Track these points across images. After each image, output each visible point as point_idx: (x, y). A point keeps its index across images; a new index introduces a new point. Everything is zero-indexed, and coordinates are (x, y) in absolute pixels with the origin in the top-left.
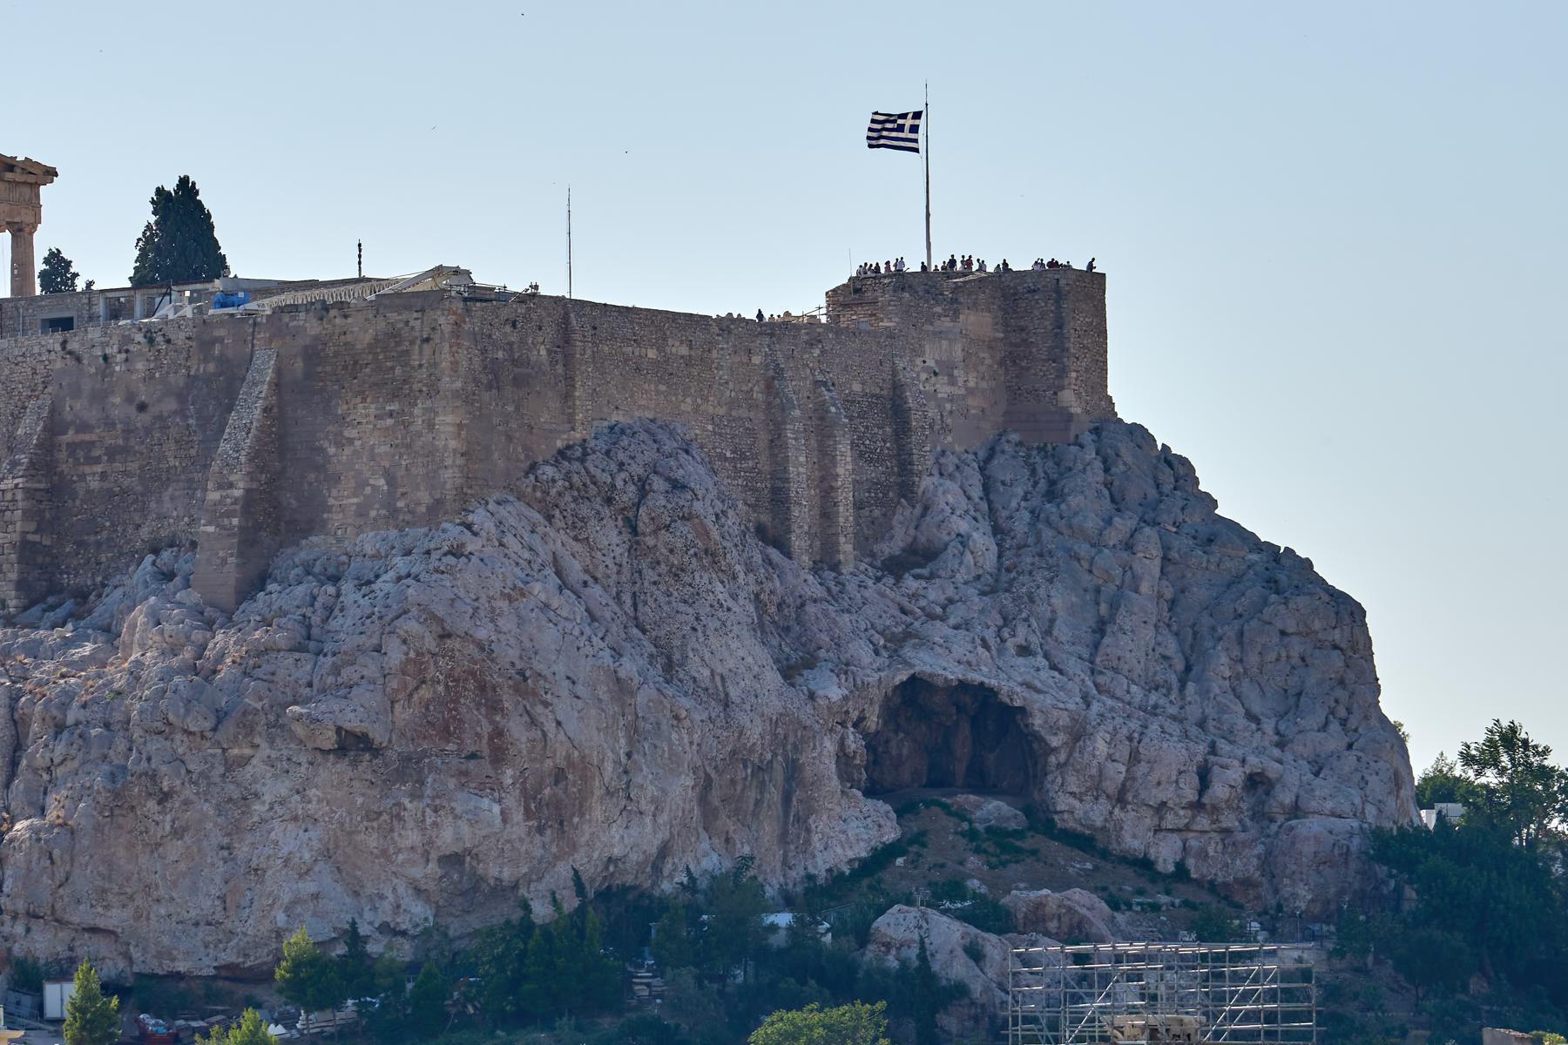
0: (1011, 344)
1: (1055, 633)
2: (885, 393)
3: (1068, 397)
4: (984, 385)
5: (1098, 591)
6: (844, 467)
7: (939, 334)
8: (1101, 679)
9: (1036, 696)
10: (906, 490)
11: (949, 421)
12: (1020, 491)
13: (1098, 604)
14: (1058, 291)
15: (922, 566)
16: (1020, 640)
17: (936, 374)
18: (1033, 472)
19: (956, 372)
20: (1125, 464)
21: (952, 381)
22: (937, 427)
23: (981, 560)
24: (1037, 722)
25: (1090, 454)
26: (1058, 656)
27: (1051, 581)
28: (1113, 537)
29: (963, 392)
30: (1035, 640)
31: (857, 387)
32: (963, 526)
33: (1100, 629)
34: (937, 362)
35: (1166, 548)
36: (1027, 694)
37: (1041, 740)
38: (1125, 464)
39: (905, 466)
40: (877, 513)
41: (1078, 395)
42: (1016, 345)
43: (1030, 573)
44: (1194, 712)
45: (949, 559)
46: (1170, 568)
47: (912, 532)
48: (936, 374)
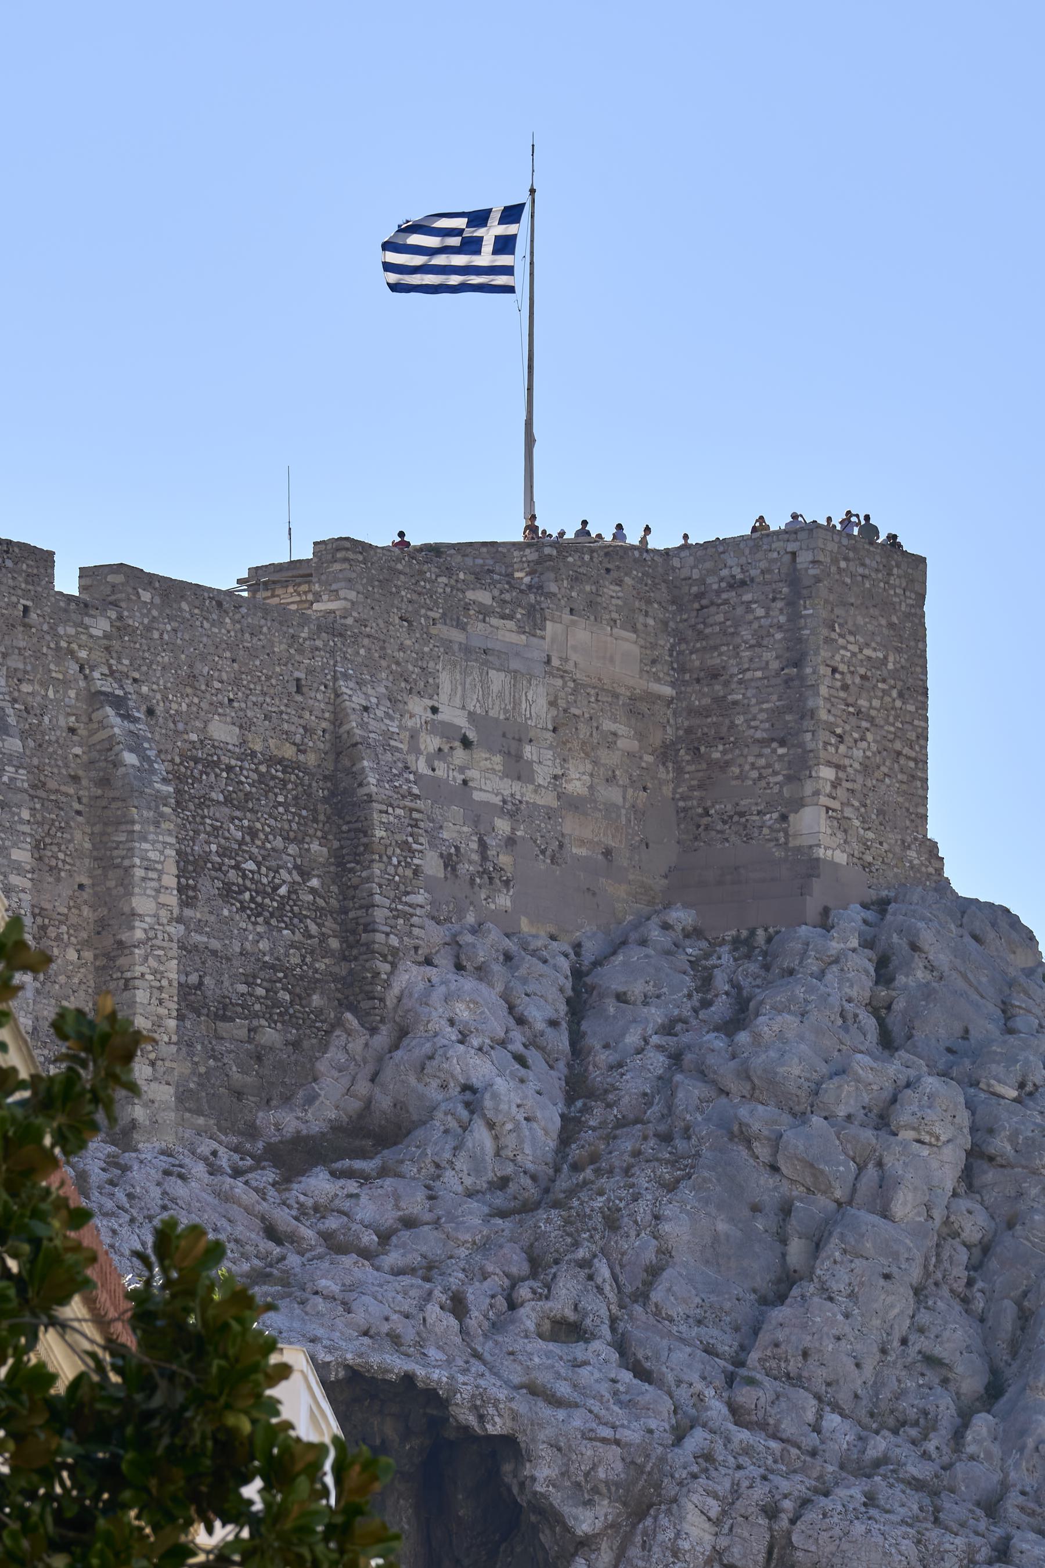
0: (691, 712)
1: (656, 1296)
2: (311, 759)
3: (812, 824)
4: (613, 794)
5: (786, 1210)
6: (153, 902)
7: (486, 656)
8: (745, 1396)
9: (546, 1411)
10: (358, 994)
11: (505, 860)
12: (656, 1015)
13: (784, 1242)
14: (794, 579)
15: (363, 1155)
16: (561, 1305)
17: (466, 743)
18: (706, 982)
20: (930, 968)
21: (517, 768)
22: (465, 868)
23: (510, 1141)
24: (543, 1472)
25: (846, 938)
26: (648, 1344)
27: (671, 1187)
28: (846, 1098)
29: (548, 799)
30: (598, 1309)
31: (222, 731)
32: (480, 1069)
33: (783, 1286)
34: (472, 716)
35: (981, 1130)
36: (521, 1405)
37: (552, 1517)
38: (930, 968)
39: (356, 934)
40: (270, 1035)
41: (841, 824)
42: (704, 712)
43: (627, 1171)
44: (977, 1475)
45: (433, 1141)
46: (990, 1175)
47: (363, 1087)
48: (466, 743)
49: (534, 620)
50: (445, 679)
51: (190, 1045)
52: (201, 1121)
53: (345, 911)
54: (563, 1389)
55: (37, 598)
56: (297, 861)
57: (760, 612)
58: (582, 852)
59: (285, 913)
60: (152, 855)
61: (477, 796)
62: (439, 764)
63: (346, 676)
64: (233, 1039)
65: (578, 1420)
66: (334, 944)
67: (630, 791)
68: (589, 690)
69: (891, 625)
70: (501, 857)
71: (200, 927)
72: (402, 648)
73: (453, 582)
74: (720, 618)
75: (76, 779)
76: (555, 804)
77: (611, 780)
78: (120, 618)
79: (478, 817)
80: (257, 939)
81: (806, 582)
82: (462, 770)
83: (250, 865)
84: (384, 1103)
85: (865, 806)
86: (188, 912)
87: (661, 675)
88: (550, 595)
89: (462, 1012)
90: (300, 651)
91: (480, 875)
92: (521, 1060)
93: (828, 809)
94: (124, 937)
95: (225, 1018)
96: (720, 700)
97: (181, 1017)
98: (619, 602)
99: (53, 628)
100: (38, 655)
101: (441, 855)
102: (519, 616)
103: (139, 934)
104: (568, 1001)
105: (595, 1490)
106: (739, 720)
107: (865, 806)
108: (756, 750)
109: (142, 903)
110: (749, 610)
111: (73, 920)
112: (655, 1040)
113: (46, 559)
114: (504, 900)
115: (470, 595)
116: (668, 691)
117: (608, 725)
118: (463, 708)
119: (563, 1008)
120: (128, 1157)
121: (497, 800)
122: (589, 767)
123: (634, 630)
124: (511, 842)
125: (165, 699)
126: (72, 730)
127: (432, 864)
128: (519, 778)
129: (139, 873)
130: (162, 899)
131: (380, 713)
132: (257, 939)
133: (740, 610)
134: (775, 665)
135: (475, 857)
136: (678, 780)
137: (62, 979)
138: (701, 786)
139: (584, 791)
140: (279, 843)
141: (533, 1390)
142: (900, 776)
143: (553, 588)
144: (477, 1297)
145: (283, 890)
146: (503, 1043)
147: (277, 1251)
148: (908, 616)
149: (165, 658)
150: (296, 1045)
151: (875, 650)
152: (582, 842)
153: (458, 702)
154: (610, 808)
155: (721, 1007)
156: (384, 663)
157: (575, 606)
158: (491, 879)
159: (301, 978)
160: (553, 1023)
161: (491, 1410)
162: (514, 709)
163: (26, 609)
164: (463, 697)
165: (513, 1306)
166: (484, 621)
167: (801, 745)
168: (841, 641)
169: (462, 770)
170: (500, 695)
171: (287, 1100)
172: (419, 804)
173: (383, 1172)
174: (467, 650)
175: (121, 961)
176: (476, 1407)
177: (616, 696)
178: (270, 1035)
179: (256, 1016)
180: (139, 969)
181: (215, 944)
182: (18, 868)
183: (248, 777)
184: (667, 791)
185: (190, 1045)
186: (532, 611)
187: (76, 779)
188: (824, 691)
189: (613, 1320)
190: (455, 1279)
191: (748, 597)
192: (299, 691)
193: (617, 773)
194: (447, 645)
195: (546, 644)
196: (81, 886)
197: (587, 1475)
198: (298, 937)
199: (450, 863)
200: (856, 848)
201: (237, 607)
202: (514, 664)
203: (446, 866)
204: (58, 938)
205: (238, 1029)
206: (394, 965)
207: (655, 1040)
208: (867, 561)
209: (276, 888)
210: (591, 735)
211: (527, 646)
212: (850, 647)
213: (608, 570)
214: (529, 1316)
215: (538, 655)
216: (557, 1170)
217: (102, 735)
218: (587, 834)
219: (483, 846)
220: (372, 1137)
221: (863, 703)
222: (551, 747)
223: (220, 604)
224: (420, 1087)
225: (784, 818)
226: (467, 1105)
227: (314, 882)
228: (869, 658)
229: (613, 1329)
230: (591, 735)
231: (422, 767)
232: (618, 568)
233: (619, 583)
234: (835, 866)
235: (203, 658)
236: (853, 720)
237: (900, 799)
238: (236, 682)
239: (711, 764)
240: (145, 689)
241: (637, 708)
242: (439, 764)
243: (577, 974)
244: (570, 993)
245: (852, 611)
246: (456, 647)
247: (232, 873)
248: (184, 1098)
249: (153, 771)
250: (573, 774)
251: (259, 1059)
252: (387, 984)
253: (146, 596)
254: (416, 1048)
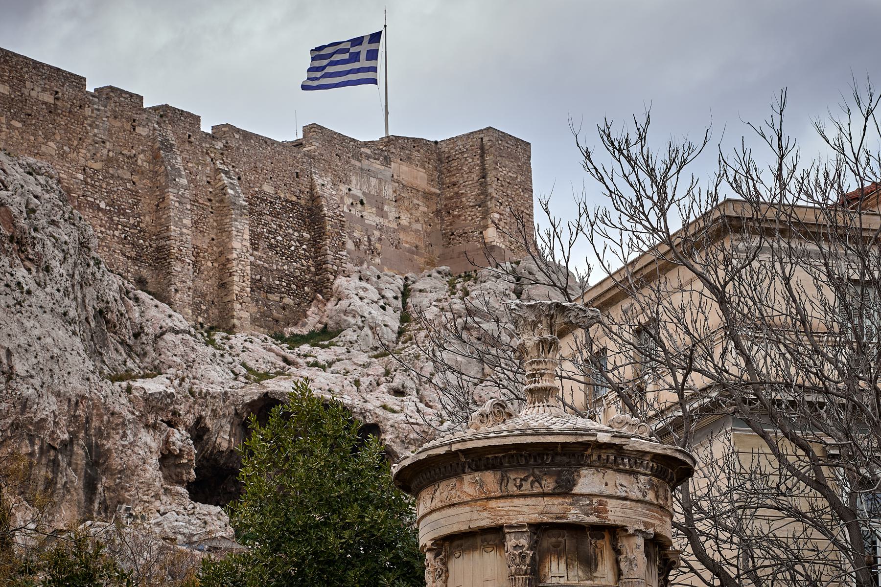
0: (447, 199)
2: (303, 202)
4: (418, 226)
6: (240, 244)
9: (390, 415)
11: (377, 245)
12: (434, 296)
16: (396, 383)
17: (362, 203)
19: (386, 208)
22: (362, 247)
29: (394, 225)
31: (268, 188)
39: (320, 267)
40: (288, 300)
41: (502, 233)
42: (451, 198)
45: (350, 335)
49: (387, 161)
50: (353, 178)
51: (257, 301)
52: (262, 329)
53: (317, 257)
54: (397, 408)
55: (193, 132)
56: (297, 237)
57: (470, 160)
58: (407, 246)
59: (292, 257)
60: (239, 227)
61: (366, 221)
62: (353, 209)
63: (315, 173)
64: (274, 301)
65: (402, 417)
66: (313, 269)
69: (518, 166)
71: (260, 259)
72: (337, 166)
74: (456, 164)
75: (210, 200)
77: (417, 221)
78: (227, 143)
79: (367, 230)
80: (281, 265)
81: (487, 148)
82: (361, 212)
83: (280, 238)
84: (331, 323)
86: (256, 253)
88: (393, 153)
89: (362, 293)
90: (298, 162)
91: (369, 250)
92: (383, 308)
94: (229, 257)
95: (271, 293)
96: (456, 193)
97: (252, 290)
99: (200, 144)
100: (194, 153)
103: (235, 256)
104: (402, 293)
105: (409, 443)
106: (464, 199)
108: (470, 209)
109: (236, 244)
110: (466, 160)
111: (210, 251)
112: (434, 303)
113: (198, 119)
114: (378, 260)
115: (363, 150)
116: (438, 192)
117: (415, 201)
119: (400, 295)
120: (230, 336)
121: (375, 224)
124: (380, 239)
125: (245, 174)
126: (209, 182)
127: (350, 245)
129: (235, 233)
130: (244, 243)
131: (328, 187)
132: (281, 265)
133: (463, 160)
134: (476, 178)
135: (367, 243)
136: (442, 223)
137: (206, 273)
138: (451, 224)
139: (407, 224)
140: (291, 231)
141: (384, 407)
143: (394, 150)
144: (365, 381)
145: (293, 248)
146: (376, 303)
147: (288, 367)
148: (524, 163)
149: (245, 159)
150: (299, 304)
152: (407, 243)
153: (358, 187)
154: (417, 231)
155: (460, 294)
159: (300, 280)
160: (396, 298)
161: (368, 414)
163: (190, 136)
165: (378, 385)
167: (487, 206)
169: (361, 212)
170: (375, 186)
171: (295, 324)
172: (343, 219)
173: (332, 344)
174: (362, 169)
175: (228, 266)
176: (361, 413)
177: (418, 191)
178: (288, 300)
179: (283, 293)
180: (235, 269)
181: (266, 265)
182: (185, 226)
183: (278, 207)
184: (438, 227)
185: (257, 301)
186: (386, 158)
187: (210, 200)
188: (494, 186)
189: (418, 391)
190: (356, 376)
191: (465, 156)
192: (297, 177)
194: (354, 166)
195: (391, 170)
196: (213, 239)
197: (406, 437)
198: (299, 265)
199: (357, 244)
200: (508, 244)
201: (273, 144)
202: (379, 176)
204: (204, 257)
205: (275, 297)
206: (335, 277)
207: (434, 303)
209: (290, 247)
214: (383, 388)
215: (389, 174)
216: (397, 344)
217: (220, 184)
218: (409, 239)
219: (369, 240)
220: (325, 335)
221: (509, 192)
222: (395, 207)
223: (266, 142)
224: (345, 318)
225: (481, 233)
226: (363, 321)
227: (304, 247)
229: (418, 394)
231: (345, 209)
233: (418, 151)
234: (500, 248)
235: (260, 161)
238: (273, 171)
239: (454, 216)
240: (237, 170)
241: (427, 196)
242: (353, 209)
243: (406, 286)
244: (402, 289)
247: (272, 241)
248: (254, 320)
249: (239, 197)
250: (402, 217)
251: (284, 309)
252: (332, 284)
253: (237, 136)
254: (344, 304)
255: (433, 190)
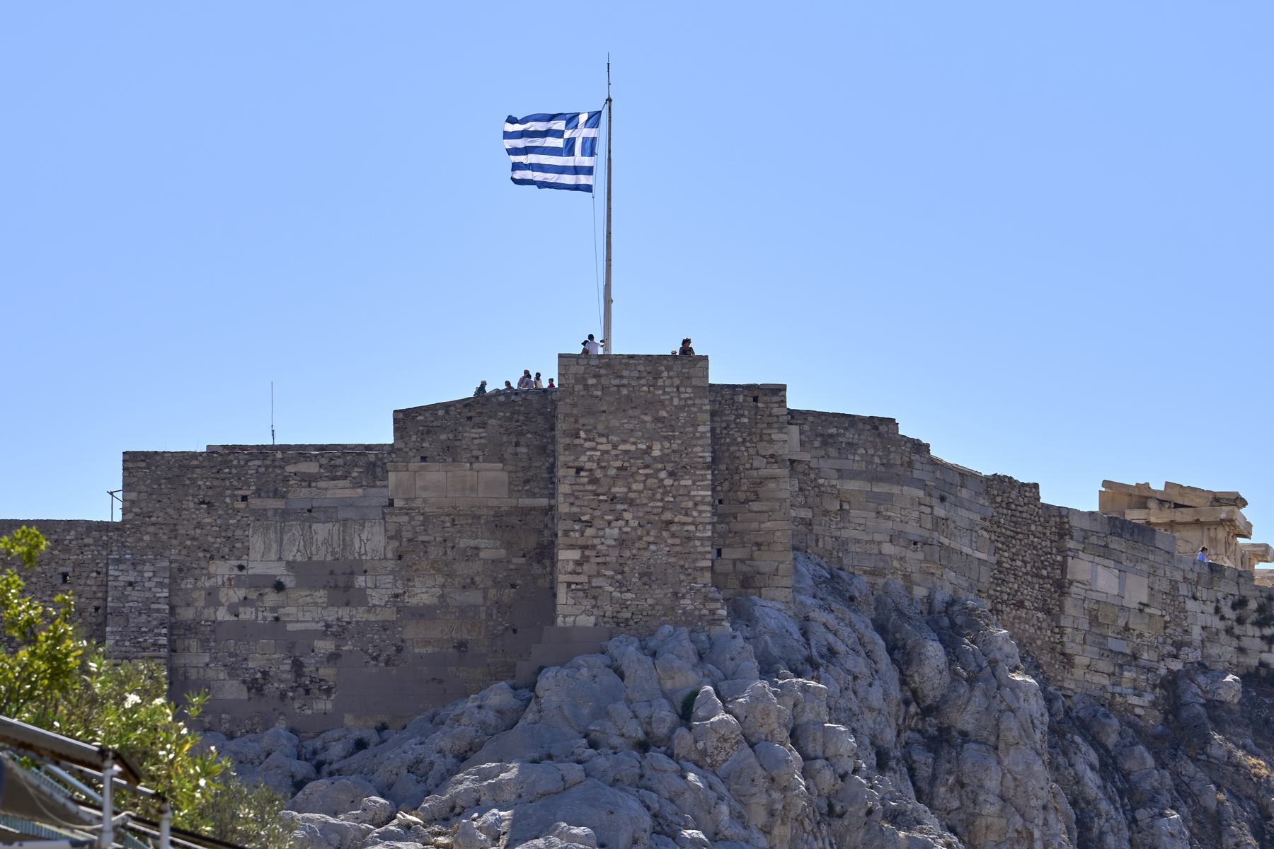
4: (473, 597)
17: (279, 587)
61: (290, 627)
67: (492, 592)
68: (442, 518)
70: (322, 671)
72: (199, 525)
73: (268, 462)
76: (394, 617)
85: (622, 573)
87: (537, 490)
93: (569, 584)
98: (483, 441)
101: (244, 682)
102: (354, 474)
107: (622, 573)
116: (544, 502)
117: (464, 543)
118: (280, 559)
122: (440, 580)
123: (502, 459)
128: (347, 604)
142: (670, 541)
151: (634, 443)
156: (174, 542)
157: (427, 454)
158: (307, 692)
162: (344, 549)
164: (280, 551)
166: (309, 486)
168: (587, 444)
169: (273, 609)
193: (477, 579)
203: (249, 690)
208: (625, 373)
210: (445, 554)
211: (364, 496)
212: (599, 447)
213: (470, 418)
228: (626, 452)
230: (445, 554)
232: (480, 414)
236: (606, 507)
237: (672, 560)
245: (603, 417)
246: (270, 514)
255: (527, 502)
